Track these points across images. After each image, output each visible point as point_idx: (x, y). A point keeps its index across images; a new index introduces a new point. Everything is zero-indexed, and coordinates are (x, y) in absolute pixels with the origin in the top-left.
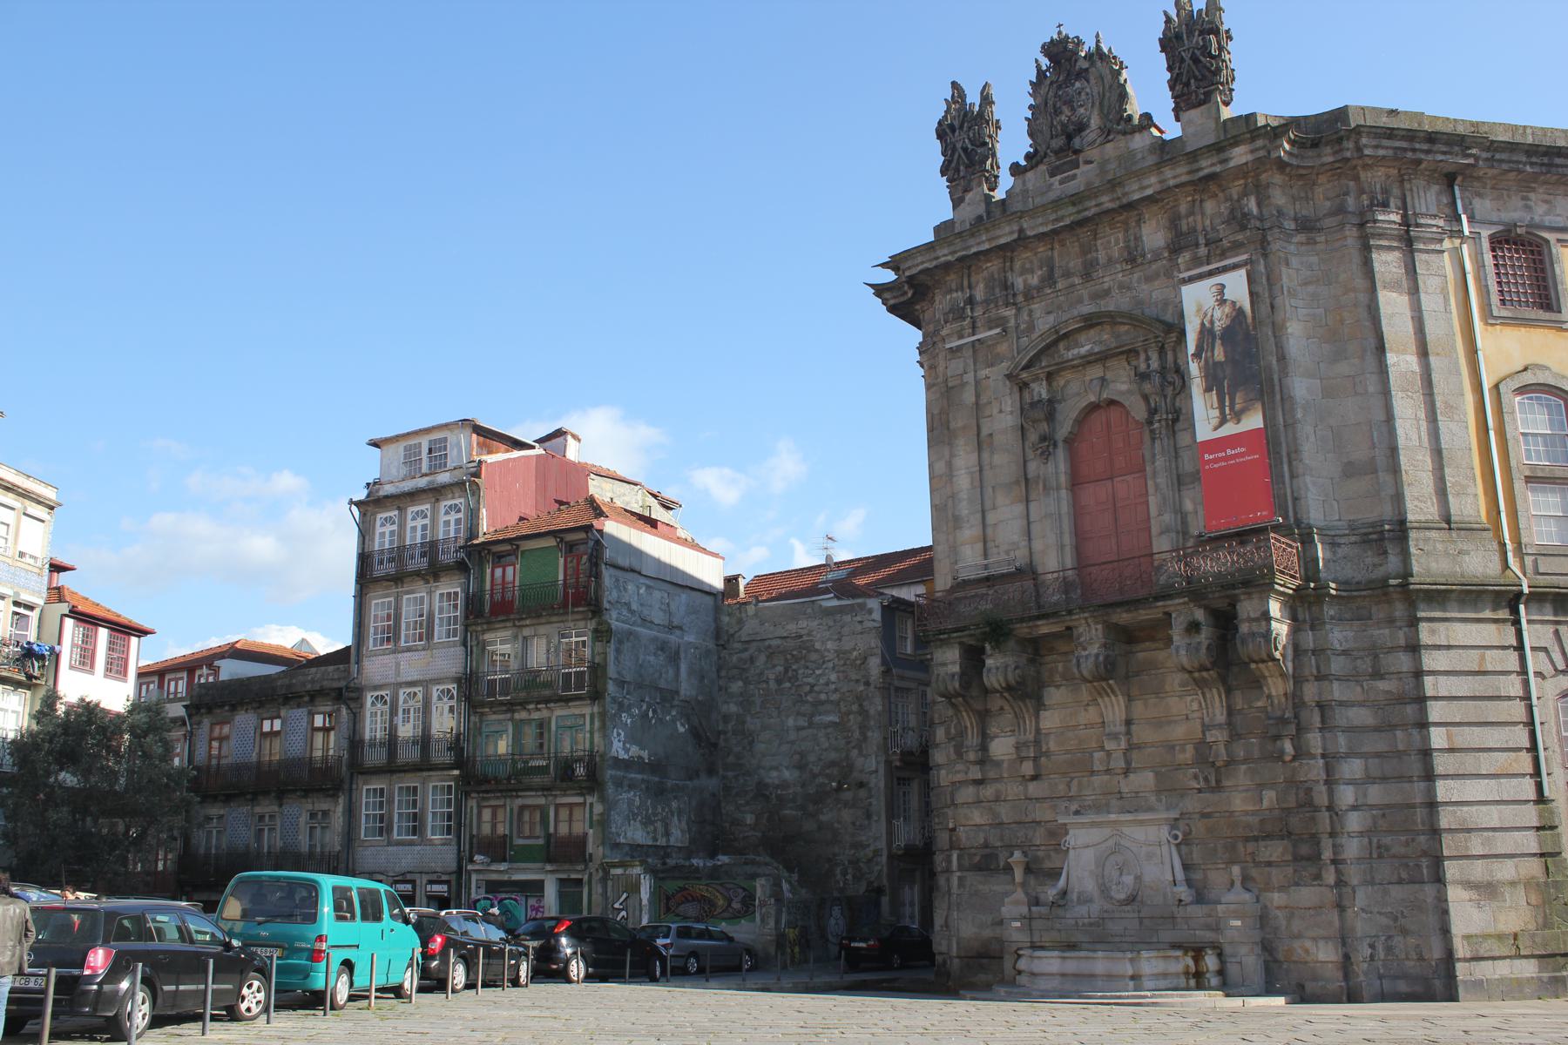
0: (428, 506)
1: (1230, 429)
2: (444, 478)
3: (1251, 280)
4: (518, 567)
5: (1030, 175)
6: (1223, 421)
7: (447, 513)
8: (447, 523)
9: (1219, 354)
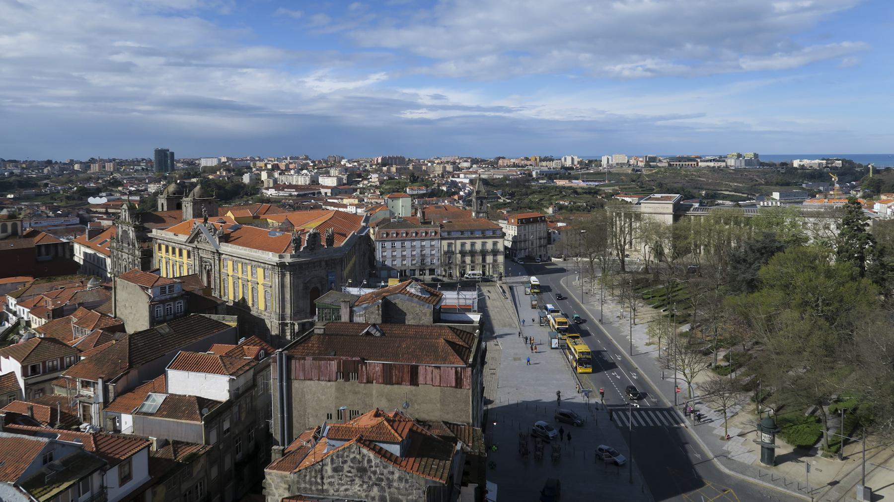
2: (175, 295)
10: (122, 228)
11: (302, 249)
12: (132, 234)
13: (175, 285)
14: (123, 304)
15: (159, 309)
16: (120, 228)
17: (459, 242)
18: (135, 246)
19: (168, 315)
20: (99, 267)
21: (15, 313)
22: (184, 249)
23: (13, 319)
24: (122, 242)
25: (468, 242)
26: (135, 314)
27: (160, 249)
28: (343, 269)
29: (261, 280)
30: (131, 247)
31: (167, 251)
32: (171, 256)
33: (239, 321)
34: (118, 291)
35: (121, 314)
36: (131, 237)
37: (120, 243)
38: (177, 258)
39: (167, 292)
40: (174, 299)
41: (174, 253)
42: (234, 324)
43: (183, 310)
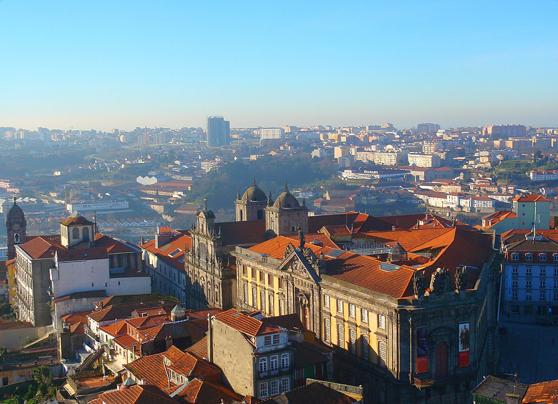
0: (277, 355)
1: (464, 350)
3: (470, 326)
4: (303, 370)
5: (432, 294)
6: (463, 349)
7: (283, 357)
8: (283, 360)
9: (464, 337)
11: (427, 293)
12: (211, 250)
13: (281, 335)
14: (221, 349)
15: (263, 362)
16: (196, 239)
18: (215, 264)
19: (273, 370)
20: (172, 282)
21: (98, 339)
22: (275, 276)
23: (97, 345)
24: (199, 256)
26: (235, 364)
27: (244, 272)
28: (477, 319)
29: (373, 327)
30: (210, 264)
31: (253, 275)
32: (258, 282)
33: (364, 393)
34: (214, 333)
36: (210, 252)
38: (267, 285)
41: (261, 278)
42: (358, 397)
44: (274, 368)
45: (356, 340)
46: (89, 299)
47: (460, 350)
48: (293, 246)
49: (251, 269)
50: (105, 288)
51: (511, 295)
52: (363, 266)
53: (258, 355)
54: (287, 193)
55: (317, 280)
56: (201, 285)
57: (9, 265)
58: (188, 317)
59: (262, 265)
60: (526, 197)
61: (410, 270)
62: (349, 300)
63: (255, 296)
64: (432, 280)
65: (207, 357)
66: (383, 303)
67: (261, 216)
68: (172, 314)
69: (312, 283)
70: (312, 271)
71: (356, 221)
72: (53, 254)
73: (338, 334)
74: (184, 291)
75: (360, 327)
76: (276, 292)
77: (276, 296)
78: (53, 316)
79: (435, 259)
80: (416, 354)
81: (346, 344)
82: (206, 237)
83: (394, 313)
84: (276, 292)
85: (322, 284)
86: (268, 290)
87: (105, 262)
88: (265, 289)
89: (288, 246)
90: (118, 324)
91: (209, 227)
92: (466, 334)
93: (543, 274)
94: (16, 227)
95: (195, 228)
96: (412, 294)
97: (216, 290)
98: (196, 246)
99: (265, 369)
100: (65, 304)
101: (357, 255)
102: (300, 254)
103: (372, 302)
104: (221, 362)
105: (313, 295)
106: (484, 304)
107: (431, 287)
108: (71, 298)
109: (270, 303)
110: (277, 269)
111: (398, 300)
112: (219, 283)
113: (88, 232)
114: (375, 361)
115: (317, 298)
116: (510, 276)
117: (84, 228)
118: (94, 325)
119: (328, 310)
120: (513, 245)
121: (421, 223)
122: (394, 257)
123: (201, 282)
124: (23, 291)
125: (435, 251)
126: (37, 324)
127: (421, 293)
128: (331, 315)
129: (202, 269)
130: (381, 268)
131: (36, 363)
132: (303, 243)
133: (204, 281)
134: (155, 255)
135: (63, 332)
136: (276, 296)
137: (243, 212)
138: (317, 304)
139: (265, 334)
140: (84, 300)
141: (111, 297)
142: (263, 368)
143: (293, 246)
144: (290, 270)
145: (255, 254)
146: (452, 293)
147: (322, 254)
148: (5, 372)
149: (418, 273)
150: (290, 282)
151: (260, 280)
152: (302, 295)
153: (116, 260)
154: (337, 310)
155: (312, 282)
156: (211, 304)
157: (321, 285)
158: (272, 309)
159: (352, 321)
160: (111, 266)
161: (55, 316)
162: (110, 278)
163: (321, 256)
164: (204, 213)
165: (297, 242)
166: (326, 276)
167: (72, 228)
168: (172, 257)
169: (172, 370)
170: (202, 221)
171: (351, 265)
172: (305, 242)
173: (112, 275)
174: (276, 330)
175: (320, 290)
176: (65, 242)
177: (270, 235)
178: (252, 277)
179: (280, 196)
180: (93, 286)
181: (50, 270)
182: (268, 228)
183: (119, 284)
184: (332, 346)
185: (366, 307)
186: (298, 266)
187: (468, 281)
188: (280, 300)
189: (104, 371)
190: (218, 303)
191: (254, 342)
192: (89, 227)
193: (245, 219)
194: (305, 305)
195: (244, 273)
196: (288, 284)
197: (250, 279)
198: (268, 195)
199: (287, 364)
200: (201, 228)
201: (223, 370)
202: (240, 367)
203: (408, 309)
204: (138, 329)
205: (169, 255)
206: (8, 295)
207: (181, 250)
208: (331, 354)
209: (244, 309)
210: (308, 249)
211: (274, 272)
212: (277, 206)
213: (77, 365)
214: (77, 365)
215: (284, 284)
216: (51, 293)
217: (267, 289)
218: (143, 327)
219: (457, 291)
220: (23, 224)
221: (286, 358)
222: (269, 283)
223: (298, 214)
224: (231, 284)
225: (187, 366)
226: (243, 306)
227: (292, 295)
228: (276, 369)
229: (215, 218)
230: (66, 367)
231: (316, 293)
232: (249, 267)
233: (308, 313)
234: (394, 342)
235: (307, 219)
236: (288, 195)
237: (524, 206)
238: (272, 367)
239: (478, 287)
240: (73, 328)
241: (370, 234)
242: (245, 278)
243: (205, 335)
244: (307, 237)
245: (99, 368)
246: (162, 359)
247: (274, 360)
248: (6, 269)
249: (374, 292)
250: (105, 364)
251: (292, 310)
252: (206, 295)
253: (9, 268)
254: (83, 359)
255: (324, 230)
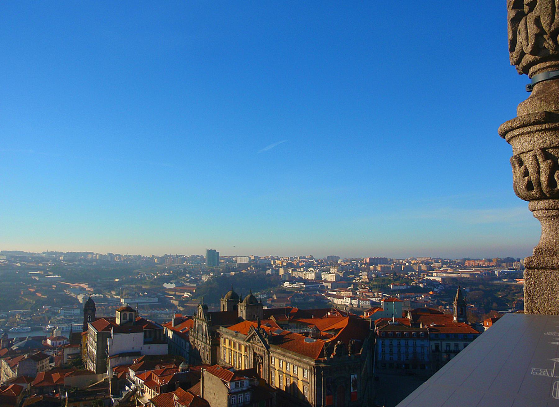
1: (354, 391)
2: (245, 389)
9: (354, 383)
10: (198, 323)
13: (245, 381)
15: (234, 398)
17: (444, 343)
18: (207, 336)
21: (134, 382)
24: (198, 332)
25: (452, 343)
26: (217, 400)
27: (225, 342)
29: (300, 377)
30: (204, 336)
31: (230, 344)
34: (205, 380)
35: (207, 397)
36: (204, 330)
37: (197, 333)
38: (237, 351)
39: (240, 386)
40: (244, 392)
41: (235, 346)
43: (249, 400)
44: (240, 402)
45: (290, 384)
46: (130, 357)
47: (352, 391)
48: (254, 327)
49: (228, 340)
50: (140, 350)
51: (382, 357)
52: (294, 339)
53: (231, 394)
54: (251, 296)
55: (268, 347)
56: (198, 349)
57: (83, 335)
58: (189, 369)
59: (235, 338)
60: (388, 299)
61: (322, 342)
62: (286, 360)
63: (230, 356)
64: (335, 348)
65: (200, 395)
66: (306, 362)
67: (235, 309)
68: (180, 367)
69: (264, 349)
70: (265, 343)
71: (291, 312)
72: (110, 329)
73: (280, 381)
74: (188, 353)
75: (292, 377)
76: (243, 355)
77: (243, 357)
78: (108, 368)
79: (337, 336)
80: (326, 393)
81: (284, 387)
82: (202, 320)
83: (313, 368)
84: (243, 355)
85: (270, 350)
86: (238, 353)
87: (141, 335)
88: (236, 353)
89: (251, 327)
90: (147, 373)
91: (205, 314)
92: (355, 381)
93: (399, 345)
94: (90, 312)
95: (196, 315)
96: (324, 357)
97: (207, 353)
98: (197, 326)
99: (235, 402)
100: (115, 360)
101: (291, 333)
102: (258, 332)
103: (300, 361)
104: (208, 398)
105: (265, 357)
106: (366, 363)
107: (334, 352)
108: (119, 356)
109: (239, 362)
110: (244, 341)
111: (315, 360)
112: (209, 349)
113: (132, 316)
114: (301, 398)
115: (267, 358)
116: (380, 346)
117: (130, 313)
118: (132, 373)
119: (274, 366)
120: (382, 327)
121: (329, 314)
122: (313, 334)
123: (198, 348)
124: (91, 352)
125: (337, 331)
126: (98, 372)
127: (328, 356)
128: (275, 369)
129: (199, 340)
130: (305, 341)
131: (95, 397)
132: (259, 325)
133: (200, 347)
134: (172, 331)
135: (113, 378)
136: (243, 357)
137: (225, 306)
138: (267, 362)
139: (236, 381)
140: (127, 357)
141: (143, 357)
142: (234, 402)
143: (254, 327)
144: (252, 341)
145: (231, 331)
146: (347, 356)
147: (270, 332)
148: (75, 403)
149: (327, 344)
150: (251, 348)
151: (234, 347)
152: (258, 357)
153: (148, 334)
154: (279, 366)
155: (264, 349)
156: (204, 361)
157: (270, 351)
158: (240, 365)
159: (288, 373)
160: (145, 336)
161: (109, 367)
162: (144, 344)
163: (270, 333)
164: (202, 306)
165: (256, 325)
166: (273, 345)
167: (123, 313)
168: (182, 332)
169: (178, 403)
170: (200, 311)
171: (289, 338)
172: (260, 324)
173: (145, 343)
174: (242, 378)
175: (269, 353)
176: (118, 322)
177: (241, 320)
178: (229, 345)
179: (247, 297)
180: (133, 349)
181: (108, 339)
182: (239, 316)
183: (149, 348)
184: (276, 388)
185: (296, 364)
186: (257, 339)
187: (355, 349)
188: (245, 360)
189: (136, 403)
190: (208, 361)
191: (228, 385)
192: (133, 313)
193: (226, 310)
194: (260, 363)
195: (224, 343)
196: (250, 349)
197: (227, 346)
198: (239, 296)
199: (248, 400)
200: (200, 315)
201: (209, 403)
202: (220, 401)
203: (321, 366)
204: (159, 376)
205: (180, 331)
206: (81, 354)
207: (187, 328)
208: (275, 393)
209: (224, 365)
210: (263, 329)
211: (242, 342)
212: (245, 303)
213: (120, 399)
214: (120, 399)
215: (248, 350)
216: (108, 353)
217: (237, 352)
218: (162, 376)
219: (350, 355)
220: (94, 310)
221: (248, 396)
222: (239, 349)
223: (257, 308)
224: (216, 349)
225: (187, 401)
226: (223, 363)
227: (252, 357)
228: (241, 403)
229: (208, 309)
230: (113, 400)
231: (267, 355)
232: (227, 339)
233: (262, 368)
234: (312, 386)
235: (262, 311)
236: (252, 296)
237: (387, 304)
238: (239, 401)
239: (362, 352)
240: (119, 375)
241: (299, 320)
242: (225, 346)
243: (199, 381)
244: (262, 322)
245: (134, 401)
246: (173, 396)
247: (241, 397)
248: (82, 338)
249: (301, 355)
250: (138, 399)
251: (252, 366)
252: (201, 355)
253: (83, 337)
254: (124, 395)
255: (272, 318)
